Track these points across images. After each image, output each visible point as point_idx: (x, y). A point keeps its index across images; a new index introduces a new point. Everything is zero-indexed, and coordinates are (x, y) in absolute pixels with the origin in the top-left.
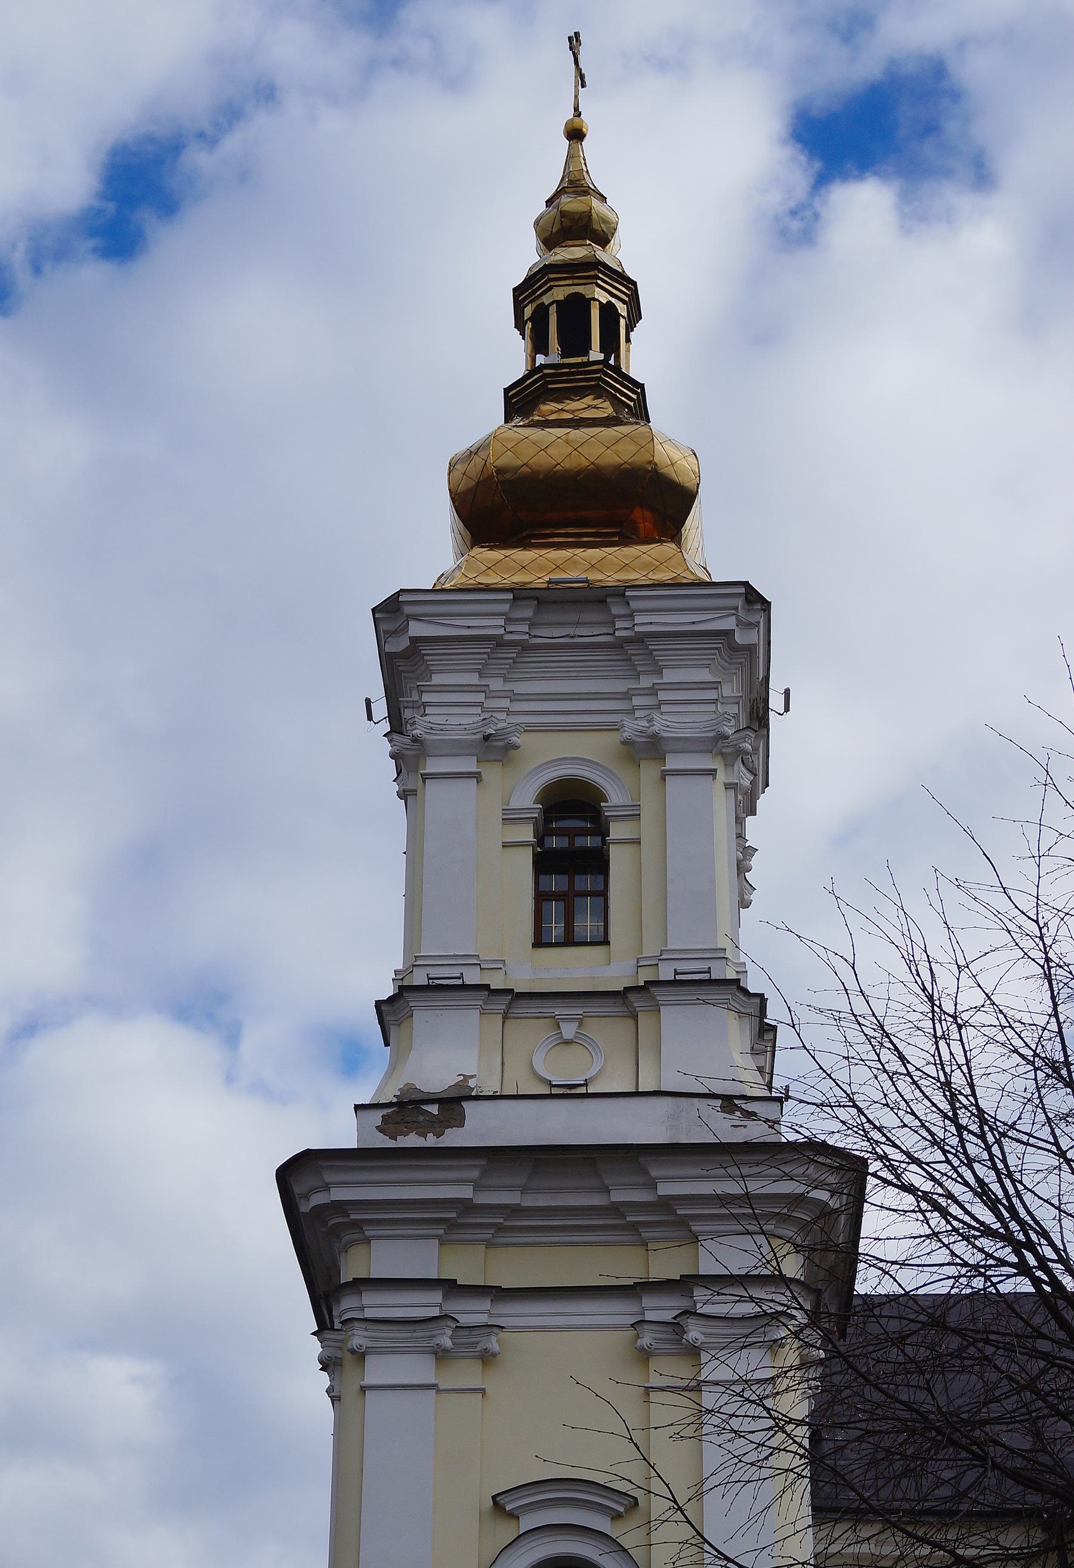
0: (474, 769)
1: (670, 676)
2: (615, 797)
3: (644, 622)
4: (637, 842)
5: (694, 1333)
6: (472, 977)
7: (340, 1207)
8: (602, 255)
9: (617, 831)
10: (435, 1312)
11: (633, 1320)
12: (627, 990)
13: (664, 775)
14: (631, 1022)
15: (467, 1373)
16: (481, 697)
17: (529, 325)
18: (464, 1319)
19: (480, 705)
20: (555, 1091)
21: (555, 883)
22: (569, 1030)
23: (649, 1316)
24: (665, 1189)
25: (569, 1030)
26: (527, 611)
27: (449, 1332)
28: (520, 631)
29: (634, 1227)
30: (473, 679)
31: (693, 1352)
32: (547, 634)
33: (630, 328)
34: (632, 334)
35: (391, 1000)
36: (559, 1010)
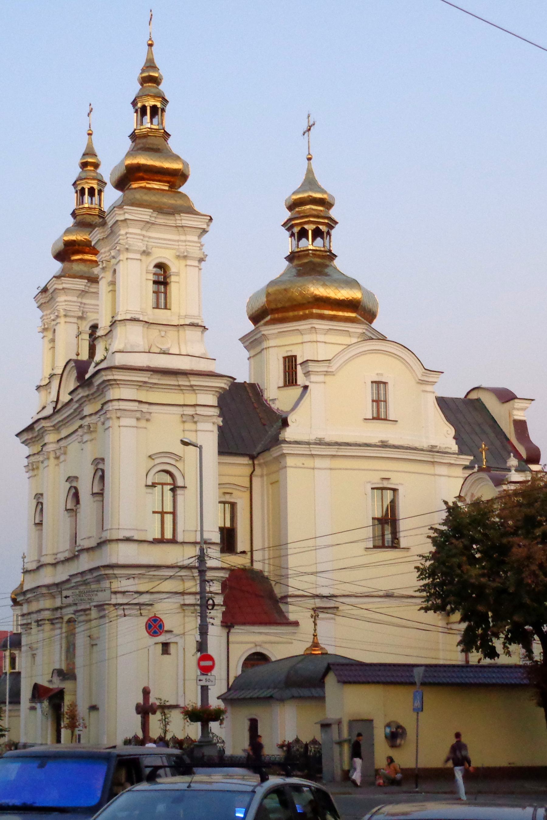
2: (173, 269)
7: (115, 380)
9: (173, 279)
11: (182, 413)
15: (143, 423)
23: (185, 413)
24: (193, 383)
25: (163, 334)
31: (196, 422)
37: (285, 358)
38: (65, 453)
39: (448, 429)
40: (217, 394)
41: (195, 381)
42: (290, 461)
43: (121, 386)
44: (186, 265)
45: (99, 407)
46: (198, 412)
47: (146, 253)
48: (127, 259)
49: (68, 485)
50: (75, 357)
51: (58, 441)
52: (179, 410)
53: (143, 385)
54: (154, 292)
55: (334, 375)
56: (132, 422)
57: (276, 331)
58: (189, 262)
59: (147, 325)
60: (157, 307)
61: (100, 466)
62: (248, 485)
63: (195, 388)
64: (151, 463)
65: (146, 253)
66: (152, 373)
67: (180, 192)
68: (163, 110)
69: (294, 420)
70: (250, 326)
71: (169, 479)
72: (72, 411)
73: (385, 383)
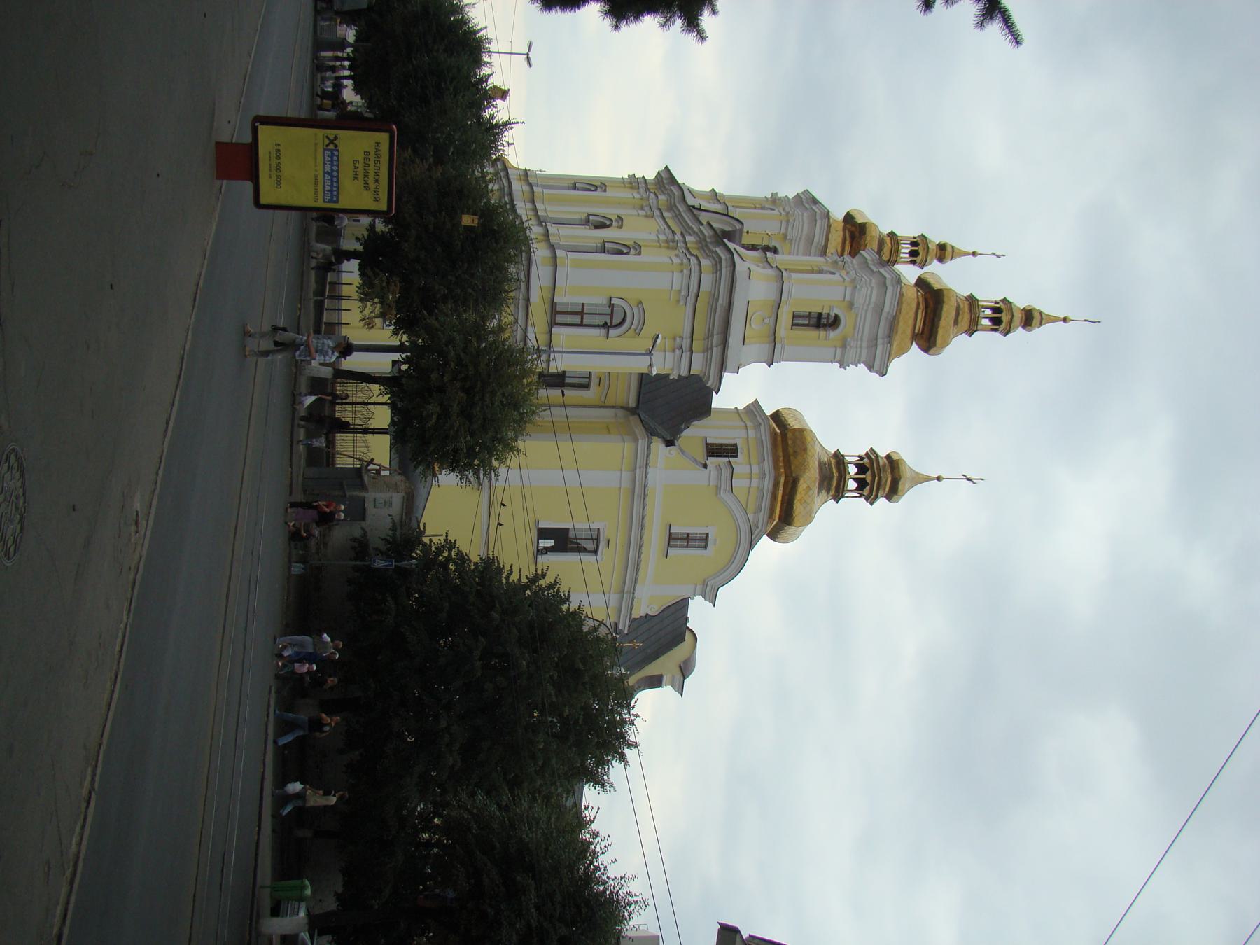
0: (846, 299)
2: (833, 334)
3: (880, 348)
7: (721, 270)
9: (823, 333)
11: (684, 337)
22: (767, 321)
23: (684, 341)
24: (715, 349)
28: (884, 314)
30: (873, 300)
37: (736, 445)
38: (646, 216)
39: (656, 609)
41: (716, 352)
42: (629, 446)
43: (715, 275)
44: (836, 348)
45: (693, 252)
46: (684, 354)
47: (851, 305)
49: (614, 218)
50: (745, 230)
51: (659, 209)
52: (687, 334)
53: (714, 297)
54: (810, 313)
55: (717, 494)
56: (676, 286)
57: (763, 437)
58: (839, 351)
60: (795, 316)
61: (632, 251)
62: (607, 403)
64: (633, 303)
67: (912, 344)
68: (995, 330)
70: (769, 412)
71: (616, 322)
72: (691, 224)
73: (705, 547)
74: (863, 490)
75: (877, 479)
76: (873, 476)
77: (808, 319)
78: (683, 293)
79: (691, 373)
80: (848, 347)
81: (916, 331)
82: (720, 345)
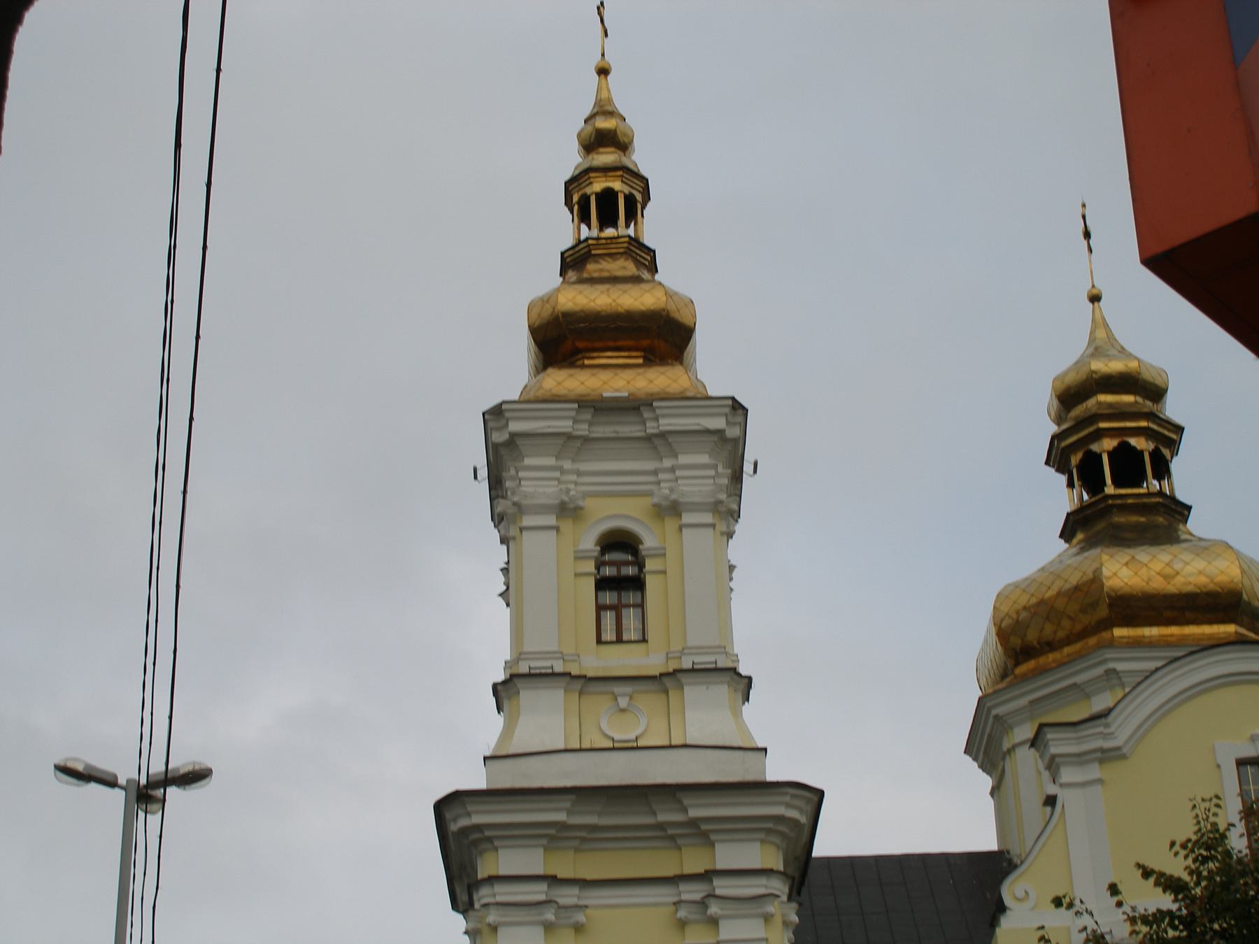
1: (683, 459)
2: (649, 542)
3: (666, 424)
4: (664, 572)
5: (714, 909)
6: (559, 667)
7: (478, 828)
8: (626, 161)
9: (650, 565)
10: (542, 897)
11: (675, 899)
12: (662, 675)
13: (681, 528)
14: (664, 696)
16: (557, 474)
17: (576, 208)
18: (562, 901)
19: (558, 479)
20: (617, 745)
21: (609, 597)
23: (685, 897)
24: (694, 813)
25: (623, 702)
26: (588, 416)
27: (553, 911)
28: (583, 429)
29: (672, 838)
30: (551, 461)
32: (601, 431)
33: (643, 208)
34: (644, 212)
35: (504, 683)
36: (619, 689)
40: (777, 840)
43: (497, 843)
46: (718, 892)
48: (521, 529)
52: (665, 895)
55: (1124, 757)
57: (1024, 701)
59: (578, 685)
63: (704, 827)
65: (567, 511)
66: (573, 797)
69: (1020, 894)
74: (1142, 452)
75: (1103, 425)
76: (1099, 435)
77: (624, 612)
78: (550, 916)
79: (781, 868)
80: (674, 497)
81: (640, 361)
82: (680, 802)
